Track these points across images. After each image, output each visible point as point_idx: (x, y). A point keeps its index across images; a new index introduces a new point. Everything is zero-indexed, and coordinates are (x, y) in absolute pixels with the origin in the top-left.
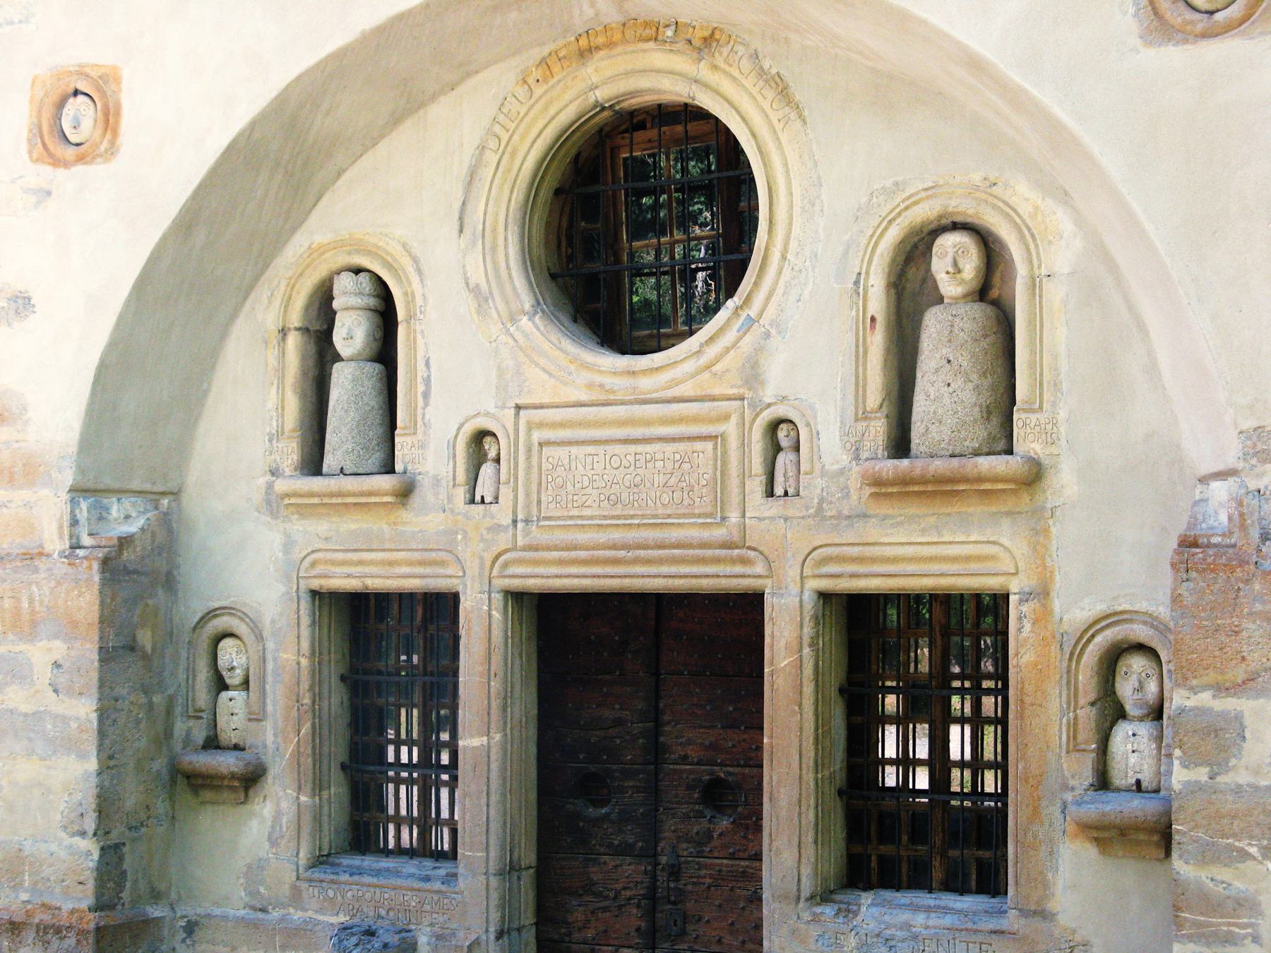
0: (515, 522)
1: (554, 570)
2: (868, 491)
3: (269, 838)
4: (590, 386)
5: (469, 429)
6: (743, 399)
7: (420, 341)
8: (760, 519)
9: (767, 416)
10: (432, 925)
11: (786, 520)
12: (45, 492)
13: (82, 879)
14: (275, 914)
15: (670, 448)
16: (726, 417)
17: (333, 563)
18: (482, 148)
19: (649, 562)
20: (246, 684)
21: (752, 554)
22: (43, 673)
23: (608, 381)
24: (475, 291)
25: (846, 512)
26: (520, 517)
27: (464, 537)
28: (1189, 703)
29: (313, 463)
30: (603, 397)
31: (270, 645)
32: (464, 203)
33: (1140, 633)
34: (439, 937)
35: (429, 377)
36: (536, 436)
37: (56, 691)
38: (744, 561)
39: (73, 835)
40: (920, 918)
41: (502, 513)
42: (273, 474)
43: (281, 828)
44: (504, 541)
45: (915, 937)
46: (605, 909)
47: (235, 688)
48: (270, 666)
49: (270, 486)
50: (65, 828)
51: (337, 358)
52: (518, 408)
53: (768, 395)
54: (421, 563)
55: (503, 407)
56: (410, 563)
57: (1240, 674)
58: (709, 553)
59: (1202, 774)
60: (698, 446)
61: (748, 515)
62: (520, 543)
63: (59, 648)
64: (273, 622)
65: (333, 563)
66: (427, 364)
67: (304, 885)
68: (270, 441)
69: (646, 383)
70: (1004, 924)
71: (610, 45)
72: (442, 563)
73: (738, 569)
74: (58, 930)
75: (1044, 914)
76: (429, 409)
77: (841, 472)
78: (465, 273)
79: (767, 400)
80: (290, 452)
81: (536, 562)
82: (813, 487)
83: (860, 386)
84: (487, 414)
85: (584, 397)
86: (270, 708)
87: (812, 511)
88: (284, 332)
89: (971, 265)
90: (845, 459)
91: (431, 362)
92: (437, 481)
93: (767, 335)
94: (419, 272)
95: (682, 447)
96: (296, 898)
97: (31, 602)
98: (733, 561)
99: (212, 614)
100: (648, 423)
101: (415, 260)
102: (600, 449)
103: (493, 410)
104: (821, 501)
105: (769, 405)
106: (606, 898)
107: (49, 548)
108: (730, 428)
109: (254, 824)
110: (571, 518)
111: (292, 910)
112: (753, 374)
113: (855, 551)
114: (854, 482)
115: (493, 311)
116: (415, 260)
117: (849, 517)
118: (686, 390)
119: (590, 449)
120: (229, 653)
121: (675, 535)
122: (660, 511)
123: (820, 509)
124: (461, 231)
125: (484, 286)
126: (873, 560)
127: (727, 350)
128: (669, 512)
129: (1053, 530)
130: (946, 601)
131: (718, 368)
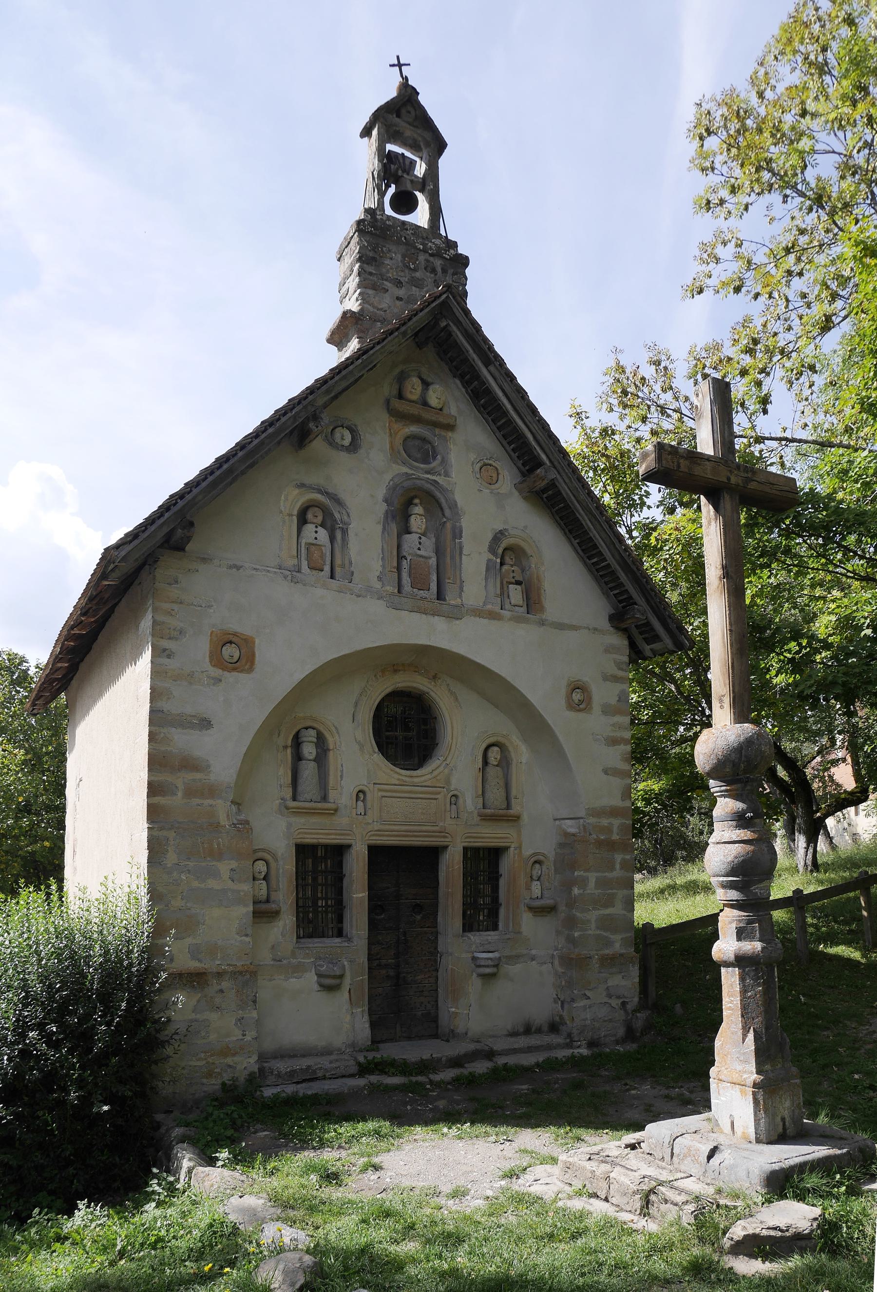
2: (479, 818)
3: (282, 934)
4: (399, 779)
5: (357, 789)
9: (452, 793)
12: (220, 801)
14: (285, 962)
16: (439, 793)
17: (306, 833)
22: (225, 874)
23: (404, 778)
24: (359, 743)
29: (294, 798)
31: (281, 863)
33: (541, 858)
36: (380, 794)
38: (446, 837)
44: (370, 828)
45: (490, 943)
47: (260, 880)
48: (281, 871)
49: (280, 804)
50: (238, 934)
53: (452, 788)
54: (340, 834)
56: (336, 834)
64: (282, 854)
65: (306, 833)
68: (281, 787)
69: (416, 780)
70: (508, 936)
72: (348, 835)
73: (442, 839)
74: (241, 973)
75: (520, 933)
80: (288, 792)
85: (397, 782)
88: (285, 747)
90: (473, 808)
92: (346, 806)
94: (338, 733)
96: (293, 955)
97: (218, 844)
100: (416, 793)
101: (336, 728)
107: (222, 823)
109: (276, 929)
112: (448, 781)
114: (475, 815)
116: (336, 728)
121: (424, 828)
126: (479, 838)
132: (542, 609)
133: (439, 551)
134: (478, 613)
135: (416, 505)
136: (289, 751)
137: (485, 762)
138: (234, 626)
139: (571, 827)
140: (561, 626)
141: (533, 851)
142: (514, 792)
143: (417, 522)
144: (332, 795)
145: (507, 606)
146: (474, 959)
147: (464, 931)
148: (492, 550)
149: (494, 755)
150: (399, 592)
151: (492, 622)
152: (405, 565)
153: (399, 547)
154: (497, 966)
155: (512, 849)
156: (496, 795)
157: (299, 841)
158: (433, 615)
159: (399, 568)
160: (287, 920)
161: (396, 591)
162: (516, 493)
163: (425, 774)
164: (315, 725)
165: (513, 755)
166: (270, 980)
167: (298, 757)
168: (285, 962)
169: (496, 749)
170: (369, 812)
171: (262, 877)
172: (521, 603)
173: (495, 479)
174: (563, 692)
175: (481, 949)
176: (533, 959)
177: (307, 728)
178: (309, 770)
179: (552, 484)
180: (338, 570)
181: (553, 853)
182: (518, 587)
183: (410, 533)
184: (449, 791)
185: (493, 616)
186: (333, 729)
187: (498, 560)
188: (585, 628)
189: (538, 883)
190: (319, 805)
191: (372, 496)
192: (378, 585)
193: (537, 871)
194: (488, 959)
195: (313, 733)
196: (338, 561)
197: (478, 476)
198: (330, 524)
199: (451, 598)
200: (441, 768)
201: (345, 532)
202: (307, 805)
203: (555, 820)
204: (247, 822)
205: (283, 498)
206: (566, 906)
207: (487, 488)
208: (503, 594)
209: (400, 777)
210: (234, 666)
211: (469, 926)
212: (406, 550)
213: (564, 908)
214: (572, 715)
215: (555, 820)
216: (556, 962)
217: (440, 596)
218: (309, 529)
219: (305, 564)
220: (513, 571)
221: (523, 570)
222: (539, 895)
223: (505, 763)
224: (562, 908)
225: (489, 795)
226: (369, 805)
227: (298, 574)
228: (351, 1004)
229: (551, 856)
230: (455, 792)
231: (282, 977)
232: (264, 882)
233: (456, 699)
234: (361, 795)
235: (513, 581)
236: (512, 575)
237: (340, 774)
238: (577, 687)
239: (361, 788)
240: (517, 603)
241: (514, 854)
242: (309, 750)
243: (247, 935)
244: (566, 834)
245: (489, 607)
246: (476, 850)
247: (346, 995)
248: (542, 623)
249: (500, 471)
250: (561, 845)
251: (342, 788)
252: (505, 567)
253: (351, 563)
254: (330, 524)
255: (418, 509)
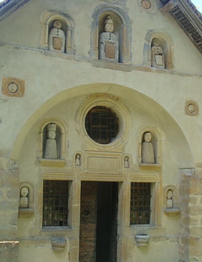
0: (84, 169)
1: (90, 177)
3: (34, 224)
4: (98, 148)
5: (76, 153)
6: (121, 153)
7: (67, 138)
8: (124, 171)
9: (125, 156)
10: (68, 237)
11: (128, 171)
13: (14, 233)
14: (36, 238)
15: (110, 159)
16: (119, 155)
17: (49, 174)
18: (79, 108)
19: (106, 176)
20: (27, 196)
21: (123, 176)
23: (100, 148)
24: (78, 131)
25: (136, 170)
26: (85, 168)
27: (75, 171)
28: (192, 196)
29: (44, 157)
30: (100, 150)
32: (75, 116)
33: (172, 188)
34: (70, 238)
35: (69, 144)
37: (8, 197)
38: (121, 177)
39: (12, 225)
40: (144, 228)
41: (82, 167)
42: (37, 158)
43: (37, 222)
46: (88, 232)
48: (35, 193)
49: (36, 160)
51: (55, 139)
52: (85, 151)
53: (126, 152)
54: (67, 175)
55: (82, 150)
56: (64, 175)
57: (196, 193)
58: (116, 175)
59: (193, 205)
60: (115, 159)
61: (122, 170)
62: (85, 172)
63: (9, 189)
66: (69, 141)
67: (42, 232)
68: (37, 152)
69: (107, 149)
71: (102, 96)
73: (120, 178)
75: (160, 225)
76: (69, 149)
77: (135, 165)
78: (76, 127)
79: (125, 153)
80: (41, 154)
81: (88, 176)
82: (132, 167)
83: (138, 152)
84: (79, 151)
85: (97, 150)
86: (35, 200)
87: (131, 170)
88: (40, 132)
89: (150, 138)
91: (70, 141)
92: (70, 161)
93: (126, 144)
94: (67, 126)
95: (112, 159)
98: (119, 177)
99: (22, 183)
102: (99, 158)
103: (80, 150)
104: (133, 168)
105: (126, 154)
106: (88, 230)
108: (119, 157)
110: (94, 169)
111: (39, 237)
112: (123, 149)
113: (137, 176)
115: (81, 134)
117: (136, 171)
118: (112, 151)
119: (97, 158)
120: (25, 191)
121: (110, 172)
122: (109, 169)
123: (133, 170)
124: (75, 120)
125: (79, 130)
127: (120, 145)
128: (110, 169)
129: (162, 174)
130: (145, 184)
131: (118, 148)
132: (172, 67)
133: (120, 40)
134: (139, 68)
135: (109, 19)
136: (42, 134)
137: (143, 141)
138: (15, 75)
139: (188, 172)
140: (182, 75)
141: (168, 184)
142: (158, 155)
143: (109, 26)
144: (63, 155)
145: (154, 65)
146: (136, 238)
147: (131, 224)
148: (147, 39)
149: (148, 137)
150: (99, 59)
151: (146, 73)
152: (102, 46)
153: (99, 38)
154: (147, 243)
155: (157, 183)
156: (149, 156)
157: (45, 178)
158: (116, 69)
159: (99, 48)
160: (38, 217)
161: (97, 58)
162: (159, 13)
163: (112, 146)
164: (55, 122)
165: (158, 137)
166: (27, 247)
167: (46, 137)
168: (36, 238)
169: (149, 134)
170: (82, 164)
171: (26, 195)
172: (162, 64)
173: (149, 6)
174: (184, 105)
175: (140, 233)
176: (167, 239)
177: (51, 124)
178: (52, 143)
179: (177, 8)
180: (68, 49)
181: (179, 185)
182: (160, 56)
183: (105, 32)
184: (124, 154)
185: (146, 70)
186: (65, 124)
187: (150, 44)
188: (195, 75)
189: (171, 200)
190: (56, 161)
191: (86, 15)
192: (88, 56)
193: (170, 194)
194: (143, 239)
195: (55, 125)
196: (68, 45)
197: (140, 5)
198: (65, 28)
199: (125, 61)
200: (120, 143)
201: (72, 32)
202: (50, 160)
203: (180, 169)
204: (17, 169)
205: (42, 16)
206: (185, 212)
207: (145, 11)
208: (153, 60)
209: (99, 147)
210: (15, 94)
211: (133, 222)
212: (103, 40)
213: (184, 213)
214: (189, 117)
215: (180, 169)
216: (180, 241)
217: (120, 61)
218: (54, 31)
219: (51, 47)
220: (158, 49)
221: (163, 49)
222: (171, 206)
223: (154, 141)
224: (183, 213)
225: (145, 156)
226: (82, 161)
227: (48, 51)
228: (70, 260)
229: (178, 187)
230: (127, 155)
231: (34, 246)
232: (27, 198)
233: (128, 109)
234: (78, 156)
235: (158, 53)
236: (157, 51)
237: (67, 145)
238: (190, 104)
239: (78, 152)
240: (160, 64)
241: (158, 186)
242: (52, 134)
243: (14, 224)
244: (185, 176)
245: (145, 66)
246: (136, 184)
247: (67, 255)
248: (172, 73)
249: (151, 3)
250: (183, 182)
251: (68, 152)
252: (154, 47)
253: (75, 46)
254: (65, 28)
255: (110, 21)
